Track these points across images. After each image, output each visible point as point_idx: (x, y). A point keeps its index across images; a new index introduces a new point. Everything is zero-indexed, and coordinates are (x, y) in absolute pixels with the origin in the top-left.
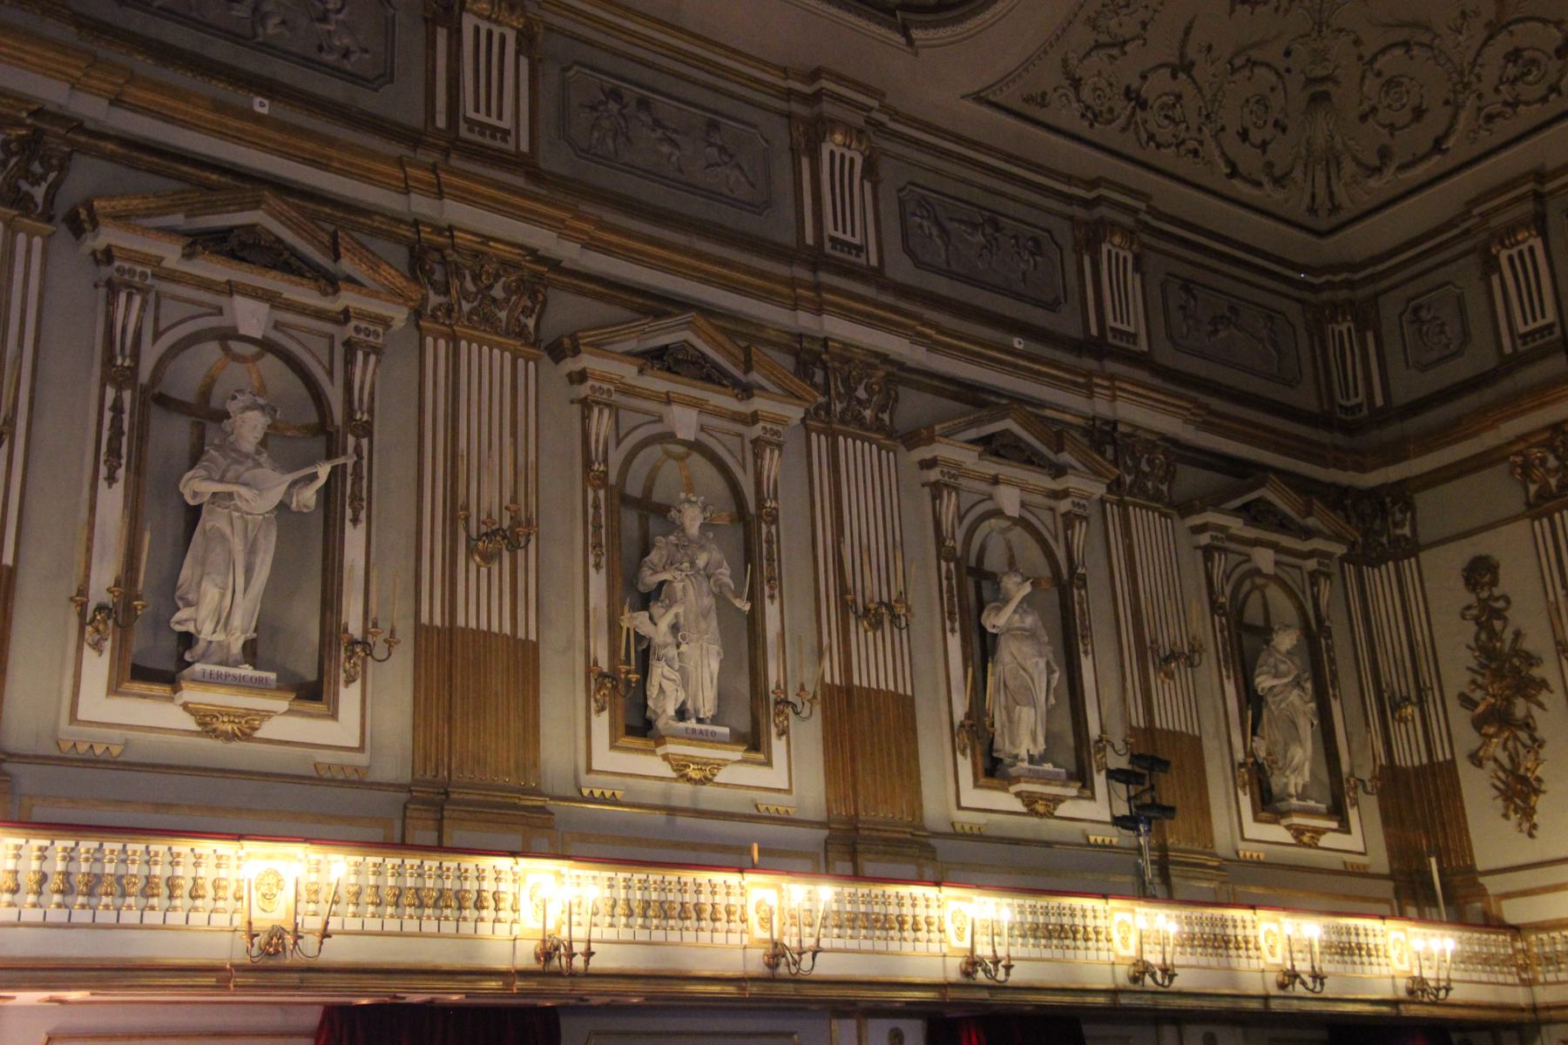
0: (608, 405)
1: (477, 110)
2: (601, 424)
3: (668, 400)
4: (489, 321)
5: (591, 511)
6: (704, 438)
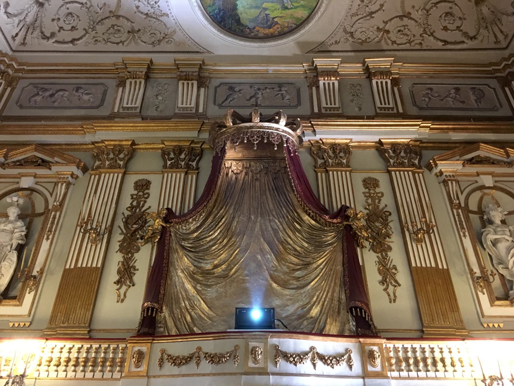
1: (381, 104)
2: (453, 187)
3: (478, 174)
4: (402, 164)
5: (456, 217)
6: (499, 185)
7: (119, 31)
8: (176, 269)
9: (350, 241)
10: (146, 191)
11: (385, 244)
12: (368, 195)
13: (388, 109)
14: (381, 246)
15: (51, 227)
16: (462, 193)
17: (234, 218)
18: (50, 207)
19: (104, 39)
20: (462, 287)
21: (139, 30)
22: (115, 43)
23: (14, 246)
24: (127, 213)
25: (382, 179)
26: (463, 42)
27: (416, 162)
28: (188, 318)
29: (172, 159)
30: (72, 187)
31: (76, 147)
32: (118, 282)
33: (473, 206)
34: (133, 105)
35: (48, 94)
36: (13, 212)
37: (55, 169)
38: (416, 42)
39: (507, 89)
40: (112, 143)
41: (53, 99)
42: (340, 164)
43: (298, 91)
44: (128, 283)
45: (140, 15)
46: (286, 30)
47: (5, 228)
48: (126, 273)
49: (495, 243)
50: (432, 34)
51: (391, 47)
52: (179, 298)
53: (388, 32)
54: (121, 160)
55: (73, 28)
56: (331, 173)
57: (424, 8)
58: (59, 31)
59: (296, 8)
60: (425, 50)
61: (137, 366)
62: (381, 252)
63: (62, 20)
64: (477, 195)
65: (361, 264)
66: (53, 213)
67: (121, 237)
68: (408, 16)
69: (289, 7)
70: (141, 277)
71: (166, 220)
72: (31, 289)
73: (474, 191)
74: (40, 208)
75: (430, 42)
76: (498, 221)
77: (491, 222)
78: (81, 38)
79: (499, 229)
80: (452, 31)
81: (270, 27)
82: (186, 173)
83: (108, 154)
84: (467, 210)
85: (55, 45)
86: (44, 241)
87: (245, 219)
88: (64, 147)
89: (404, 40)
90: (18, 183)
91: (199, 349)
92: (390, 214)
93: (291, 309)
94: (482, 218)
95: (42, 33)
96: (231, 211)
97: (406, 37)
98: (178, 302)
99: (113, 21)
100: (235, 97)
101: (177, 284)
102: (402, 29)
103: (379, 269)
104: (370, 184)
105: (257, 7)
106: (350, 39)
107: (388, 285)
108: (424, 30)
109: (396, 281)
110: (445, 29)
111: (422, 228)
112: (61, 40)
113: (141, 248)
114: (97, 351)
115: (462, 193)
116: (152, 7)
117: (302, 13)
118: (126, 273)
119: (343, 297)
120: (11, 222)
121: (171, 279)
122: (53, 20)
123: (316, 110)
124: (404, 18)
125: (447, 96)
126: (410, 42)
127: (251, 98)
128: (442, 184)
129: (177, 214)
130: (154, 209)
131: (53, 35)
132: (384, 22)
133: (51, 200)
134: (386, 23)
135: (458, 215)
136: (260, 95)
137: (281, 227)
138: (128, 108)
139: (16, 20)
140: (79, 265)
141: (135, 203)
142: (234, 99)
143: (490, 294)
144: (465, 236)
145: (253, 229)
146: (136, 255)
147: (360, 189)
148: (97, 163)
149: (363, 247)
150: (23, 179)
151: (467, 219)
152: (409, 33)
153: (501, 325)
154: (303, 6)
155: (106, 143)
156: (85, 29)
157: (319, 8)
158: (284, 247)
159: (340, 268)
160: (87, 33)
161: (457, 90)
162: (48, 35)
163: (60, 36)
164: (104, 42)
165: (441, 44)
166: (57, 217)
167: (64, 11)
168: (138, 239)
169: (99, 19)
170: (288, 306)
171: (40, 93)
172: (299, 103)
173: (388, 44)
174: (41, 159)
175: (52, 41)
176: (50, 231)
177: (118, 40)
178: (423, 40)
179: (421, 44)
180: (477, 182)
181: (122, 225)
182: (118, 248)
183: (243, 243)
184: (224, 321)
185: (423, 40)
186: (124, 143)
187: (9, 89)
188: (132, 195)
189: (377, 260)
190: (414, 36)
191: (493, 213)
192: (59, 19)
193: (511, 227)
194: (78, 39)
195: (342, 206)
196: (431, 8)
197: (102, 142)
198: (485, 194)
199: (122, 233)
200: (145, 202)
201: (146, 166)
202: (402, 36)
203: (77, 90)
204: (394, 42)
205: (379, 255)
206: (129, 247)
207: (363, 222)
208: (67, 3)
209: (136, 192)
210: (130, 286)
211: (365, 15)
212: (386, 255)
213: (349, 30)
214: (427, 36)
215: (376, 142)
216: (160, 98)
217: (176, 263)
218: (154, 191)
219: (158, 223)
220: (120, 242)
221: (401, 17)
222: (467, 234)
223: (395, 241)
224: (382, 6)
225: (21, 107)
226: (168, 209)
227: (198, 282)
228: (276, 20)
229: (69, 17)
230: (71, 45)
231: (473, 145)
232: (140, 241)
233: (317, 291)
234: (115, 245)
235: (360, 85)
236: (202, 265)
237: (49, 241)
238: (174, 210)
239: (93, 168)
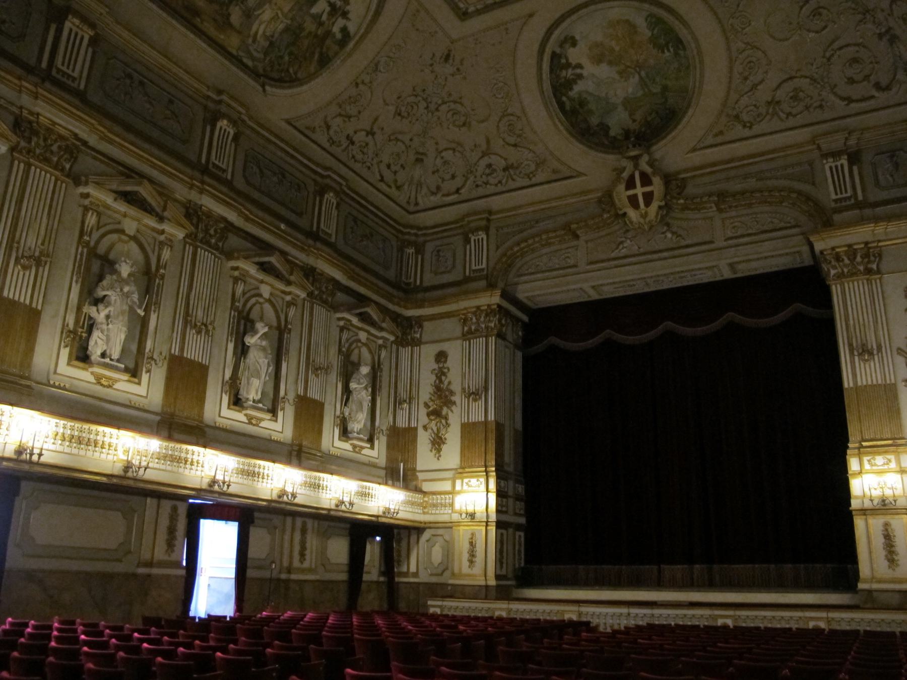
26: (873, 97)
38: (815, 105)
53: (778, 102)
55: (453, 177)
78: (463, 186)
110: (851, 81)
122: (434, 173)
131: (438, 188)
162: (434, 190)
175: (439, 196)
177: (496, 181)
187: (420, 257)
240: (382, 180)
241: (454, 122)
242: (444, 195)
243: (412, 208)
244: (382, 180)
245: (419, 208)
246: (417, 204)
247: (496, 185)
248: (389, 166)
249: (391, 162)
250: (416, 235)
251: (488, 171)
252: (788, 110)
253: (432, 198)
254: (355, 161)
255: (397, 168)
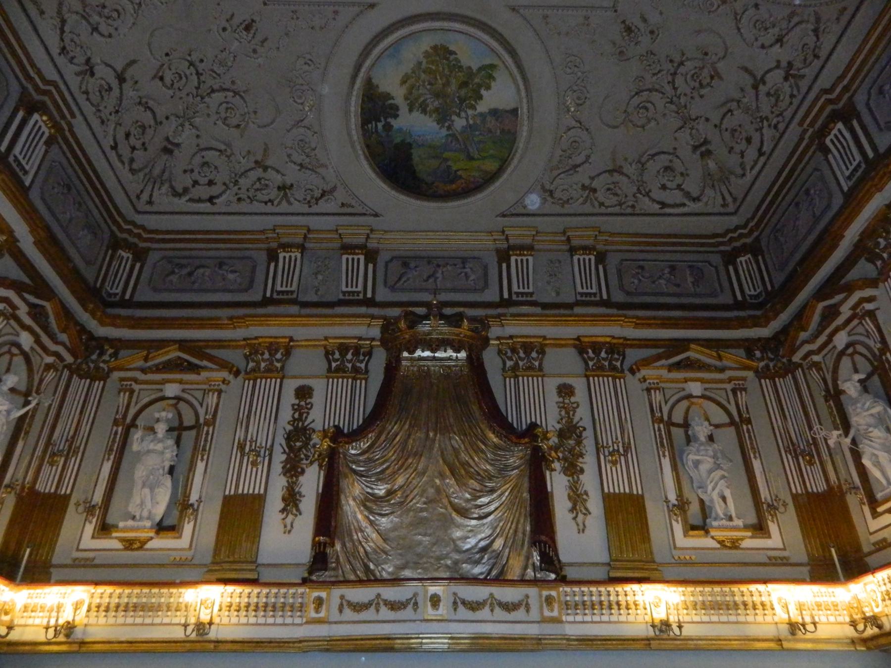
0: (659, 389)
1: (583, 288)
7: (267, 185)
8: (346, 497)
9: (537, 465)
10: (309, 401)
11: (577, 466)
12: (561, 405)
13: (590, 294)
14: (572, 469)
15: (205, 446)
16: (666, 403)
17: (409, 436)
18: (202, 420)
19: (249, 197)
20: (656, 515)
21: (292, 185)
22: (262, 202)
23: (167, 469)
24: (289, 428)
25: (579, 384)
26: (684, 205)
27: (618, 364)
28: (361, 550)
29: (337, 360)
30: (223, 395)
31: (226, 344)
32: (283, 511)
33: (678, 417)
34: (289, 289)
35: (185, 271)
36: (161, 428)
37: (204, 374)
39: (731, 268)
40: (267, 340)
41: (193, 278)
42: (530, 368)
43: (485, 268)
44: (294, 511)
45: (293, 165)
46: (472, 186)
47: (156, 448)
48: (292, 499)
49: (697, 464)
50: (647, 194)
51: (597, 210)
52: (350, 530)
53: (594, 191)
54: (278, 361)
56: (520, 378)
57: (639, 162)
58: (193, 186)
59: (484, 158)
60: (638, 215)
61: (317, 612)
62: (572, 475)
63: (196, 171)
64: (684, 404)
65: (549, 489)
66: (206, 428)
67: (284, 457)
68: (618, 170)
69: (476, 157)
70: (309, 505)
71: (334, 439)
72: (189, 518)
73: (678, 401)
74: (189, 420)
75: (646, 204)
76: (703, 438)
77: (696, 439)
79: (702, 448)
80: (671, 189)
81: (452, 182)
82: (354, 379)
83: (263, 354)
84: (670, 424)
85: (189, 204)
86: (199, 461)
87: (423, 436)
88: (210, 343)
89: (614, 200)
90: (161, 390)
91: (379, 595)
92: (585, 429)
93: (472, 542)
94: (686, 432)
95: (172, 188)
96: (407, 427)
97: (616, 198)
98: (351, 536)
99: (259, 172)
100: (410, 276)
101: (349, 514)
102: (612, 186)
103: (569, 495)
104: (565, 391)
105: (436, 157)
106: (549, 198)
107: (577, 513)
108: (638, 189)
109: (586, 509)
110: (664, 187)
111: (618, 451)
112: (196, 197)
113: (307, 470)
114: (276, 596)
115: (666, 403)
116: (307, 156)
117: (491, 166)
118: (292, 499)
119: (528, 528)
120: (160, 441)
121: (342, 509)
122: (185, 171)
123: (506, 296)
124: (615, 174)
125: (660, 277)
126: (620, 204)
127: (429, 277)
128: (645, 392)
129: (346, 431)
130: (318, 426)
131: (186, 190)
132: (590, 177)
133: (201, 411)
134: (592, 178)
135: (659, 430)
136: (439, 275)
137: (462, 446)
138: (282, 292)
139: (141, 175)
140: (240, 491)
141: (296, 415)
142: (408, 279)
143: (685, 521)
144: (664, 456)
145: (431, 449)
146: (301, 478)
147: (553, 398)
148: (251, 365)
149: (553, 470)
150: (168, 385)
151: (669, 433)
152: (619, 192)
153: (693, 557)
154: (492, 156)
155: (261, 340)
156: (225, 184)
157: (512, 159)
158: (465, 470)
159: (526, 495)
160: (228, 188)
161: (673, 268)
162: (181, 191)
163: (196, 192)
164: (249, 201)
165: (657, 206)
166: (211, 432)
167: (198, 160)
168: (302, 459)
169: (242, 170)
170: (469, 538)
171: (176, 271)
172: (486, 285)
173: (594, 206)
174: (186, 361)
176: (204, 450)
177: (266, 198)
178: (636, 201)
179: (633, 207)
180: (684, 389)
181: (284, 443)
182: (280, 470)
183: (420, 467)
184: (400, 555)
185: (636, 201)
186: (281, 340)
187: (138, 265)
188: (293, 405)
189: (568, 484)
190: (626, 196)
191: (697, 428)
192: (192, 171)
193: (715, 445)
194: (217, 197)
195: (532, 423)
196: (648, 160)
197: (256, 338)
198: (692, 403)
199: (284, 452)
200: (308, 413)
201: (307, 365)
202: (611, 196)
203: (221, 265)
204: (602, 204)
205: (570, 478)
206: (293, 469)
207: (554, 440)
208: (202, 150)
209: (297, 402)
210: (296, 515)
211: (567, 168)
212: (578, 477)
213: (547, 187)
214: (641, 196)
215: (574, 339)
216: (320, 277)
217: (347, 491)
218: (317, 399)
219: (326, 444)
220: (282, 462)
221: (610, 172)
222: (667, 453)
223: (588, 462)
224: (588, 157)
225: (155, 290)
226: (335, 426)
227: (372, 512)
228: (459, 173)
229: (205, 169)
230: (209, 204)
231: (681, 345)
232: (304, 461)
233: (500, 521)
234: (277, 467)
235: (560, 262)
236: (376, 491)
237: (204, 462)
238: (341, 426)
239: (246, 371)
240: (112, 148)
241: (226, 119)
242: (191, 200)
243: (141, 206)
244: (114, 147)
245: (154, 208)
246: (150, 202)
247: (266, 203)
248: (128, 135)
249: (133, 131)
250: (139, 236)
251: (258, 185)
252: (601, 199)
253: (176, 200)
254: (88, 99)
255: (138, 144)
